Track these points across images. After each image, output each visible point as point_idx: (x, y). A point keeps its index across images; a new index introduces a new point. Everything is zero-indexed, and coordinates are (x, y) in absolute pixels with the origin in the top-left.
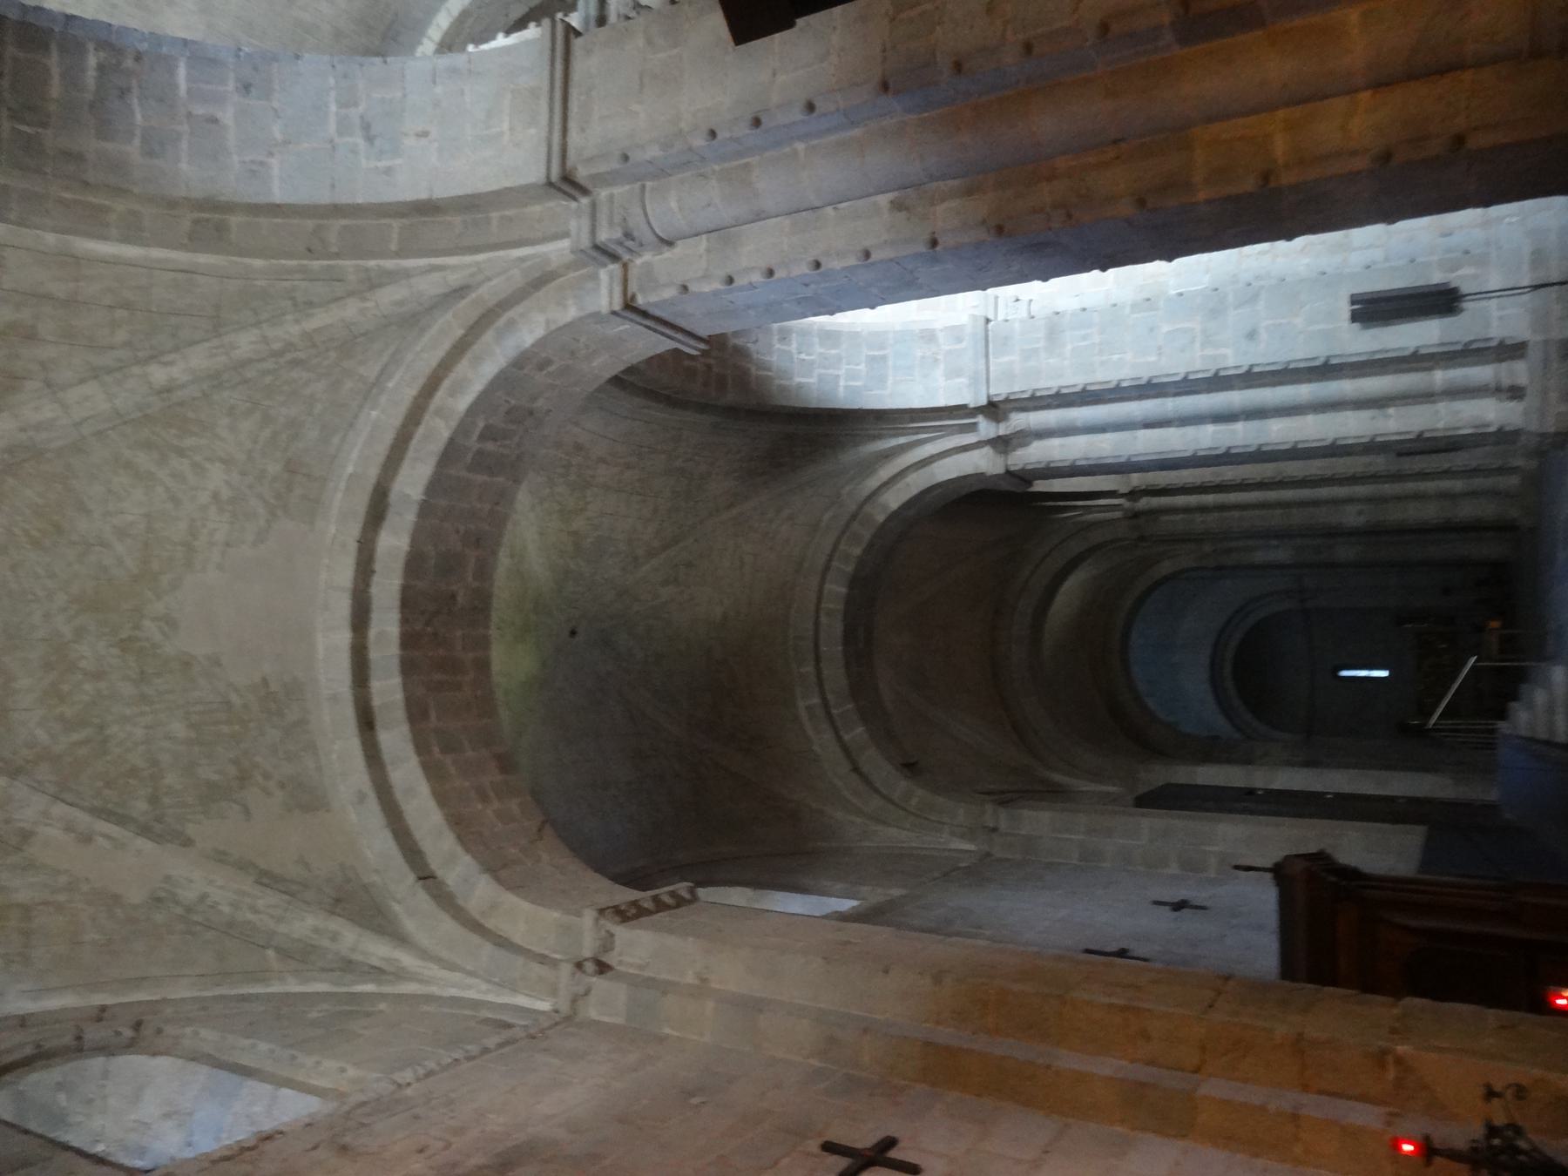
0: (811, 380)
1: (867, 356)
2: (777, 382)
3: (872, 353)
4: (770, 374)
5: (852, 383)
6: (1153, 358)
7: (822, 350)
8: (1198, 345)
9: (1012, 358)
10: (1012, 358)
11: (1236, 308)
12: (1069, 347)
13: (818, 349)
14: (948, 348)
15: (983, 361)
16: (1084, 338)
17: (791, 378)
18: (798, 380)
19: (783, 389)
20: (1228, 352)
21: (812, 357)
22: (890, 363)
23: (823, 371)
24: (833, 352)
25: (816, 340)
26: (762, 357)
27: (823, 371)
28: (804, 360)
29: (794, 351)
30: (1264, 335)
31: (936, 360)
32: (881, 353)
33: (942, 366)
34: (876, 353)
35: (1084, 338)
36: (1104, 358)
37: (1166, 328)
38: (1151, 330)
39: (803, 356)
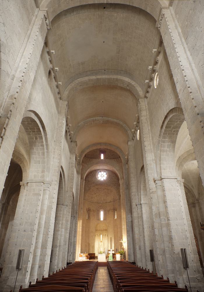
5: (35, 158)
6: (26, 213)
11: (31, 228)
13: (41, 152)
16: (34, 200)
22: (39, 165)
23: (37, 153)
25: (43, 151)
27: (37, 153)
31: (38, 173)
33: (36, 174)
35: (34, 200)
39: (39, 149)
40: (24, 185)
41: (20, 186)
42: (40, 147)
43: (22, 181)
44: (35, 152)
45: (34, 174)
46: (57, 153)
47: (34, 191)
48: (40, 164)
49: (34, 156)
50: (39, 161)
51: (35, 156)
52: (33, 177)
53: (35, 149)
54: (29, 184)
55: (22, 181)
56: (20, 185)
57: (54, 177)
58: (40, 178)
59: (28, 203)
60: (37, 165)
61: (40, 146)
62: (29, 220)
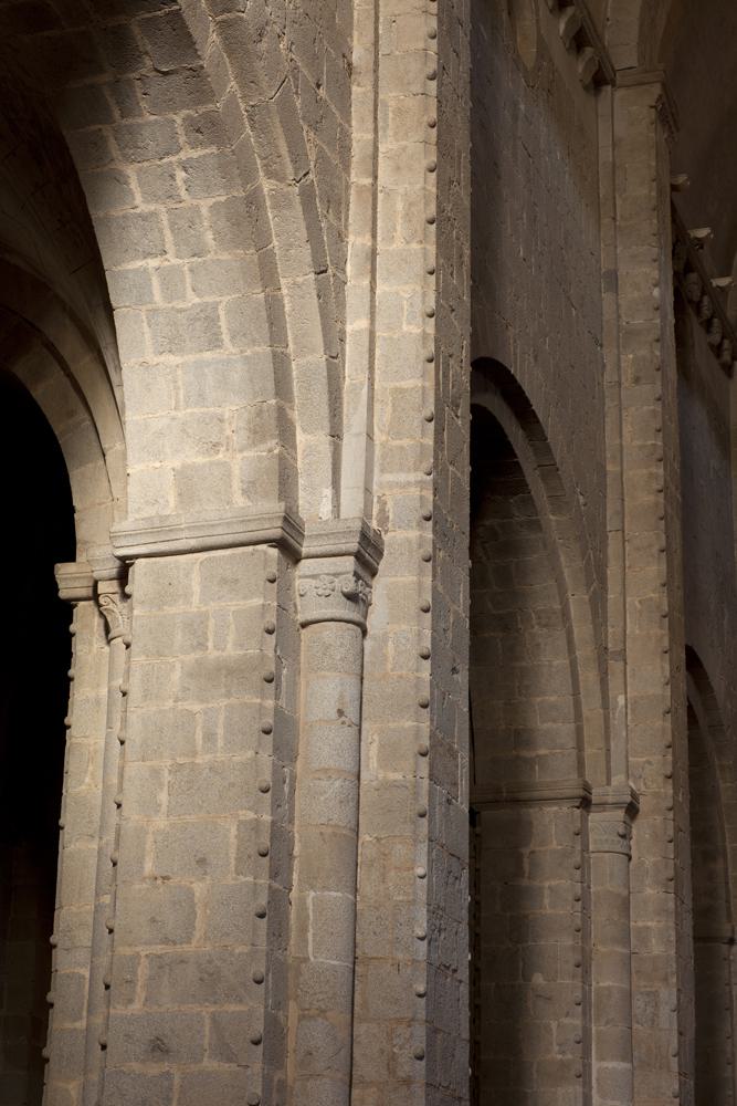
0: (138, 199)
1: (215, 307)
2: (107, 131)
3: (222, 313)
4: (117, 114)
5: (155, 282)
6: (149, 867)
7: (204, 211)
8: (158, 949)
9: (196, 599)
10: (196, 599)
12: (197, 707)
14: (236, 471)
15: (193, 543)
17: (129, 160)
18: (131, 171)
19: (97, 145)
20: (136, 1007)
21: (183, 193)
22: (208, 355)
23: (164, 219)
24: (209, 236)
26: (139, 95)
27: (164, 219)
28: (172, 177)
29: (183, 156)
30: (154, 1069)
32: (226, 337)
33: (200, 460)
34: (223, 323)
35: (210, 737)
36: (166, 777)
37: (199, 889)
38: (202, 862)
39: (181, 175)
40: (95, 597)
41: (66, 609)
42: (195, 154)
43: (71, 557)
44: (144, 217)
45: (177, 464)
46: (400, 206)
47: (202, 646)
48: (215, 343)
49: (139, 264)
50: (208, 318)
51: (153, 263)
52: (172, 500)
53: (134, 185)
54: (139, 569)
55: (71, 557)
56: (63, 594)
57: (402, 477)
58: (240, 501)
59: (156, 773)
60: (191, 358)
61: (182, 139)
62: (189, 942)
